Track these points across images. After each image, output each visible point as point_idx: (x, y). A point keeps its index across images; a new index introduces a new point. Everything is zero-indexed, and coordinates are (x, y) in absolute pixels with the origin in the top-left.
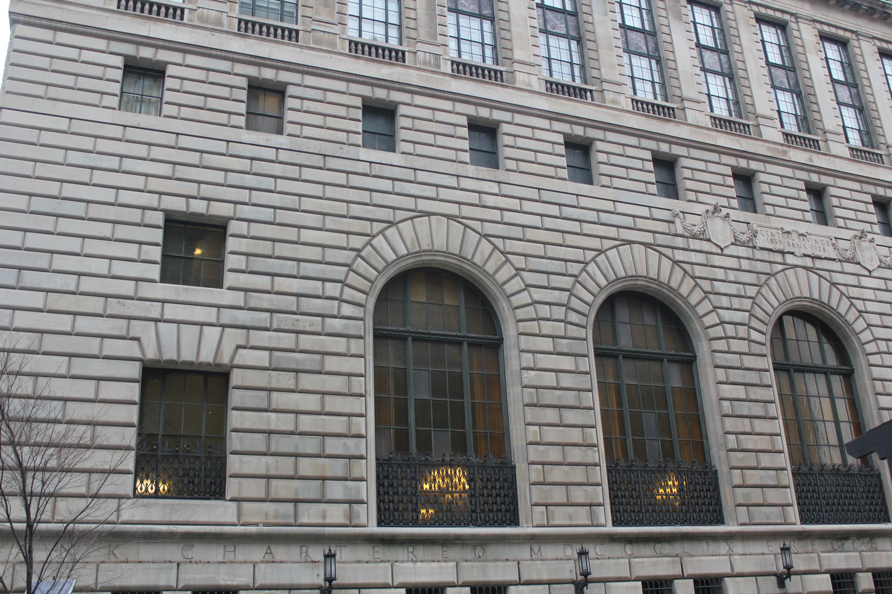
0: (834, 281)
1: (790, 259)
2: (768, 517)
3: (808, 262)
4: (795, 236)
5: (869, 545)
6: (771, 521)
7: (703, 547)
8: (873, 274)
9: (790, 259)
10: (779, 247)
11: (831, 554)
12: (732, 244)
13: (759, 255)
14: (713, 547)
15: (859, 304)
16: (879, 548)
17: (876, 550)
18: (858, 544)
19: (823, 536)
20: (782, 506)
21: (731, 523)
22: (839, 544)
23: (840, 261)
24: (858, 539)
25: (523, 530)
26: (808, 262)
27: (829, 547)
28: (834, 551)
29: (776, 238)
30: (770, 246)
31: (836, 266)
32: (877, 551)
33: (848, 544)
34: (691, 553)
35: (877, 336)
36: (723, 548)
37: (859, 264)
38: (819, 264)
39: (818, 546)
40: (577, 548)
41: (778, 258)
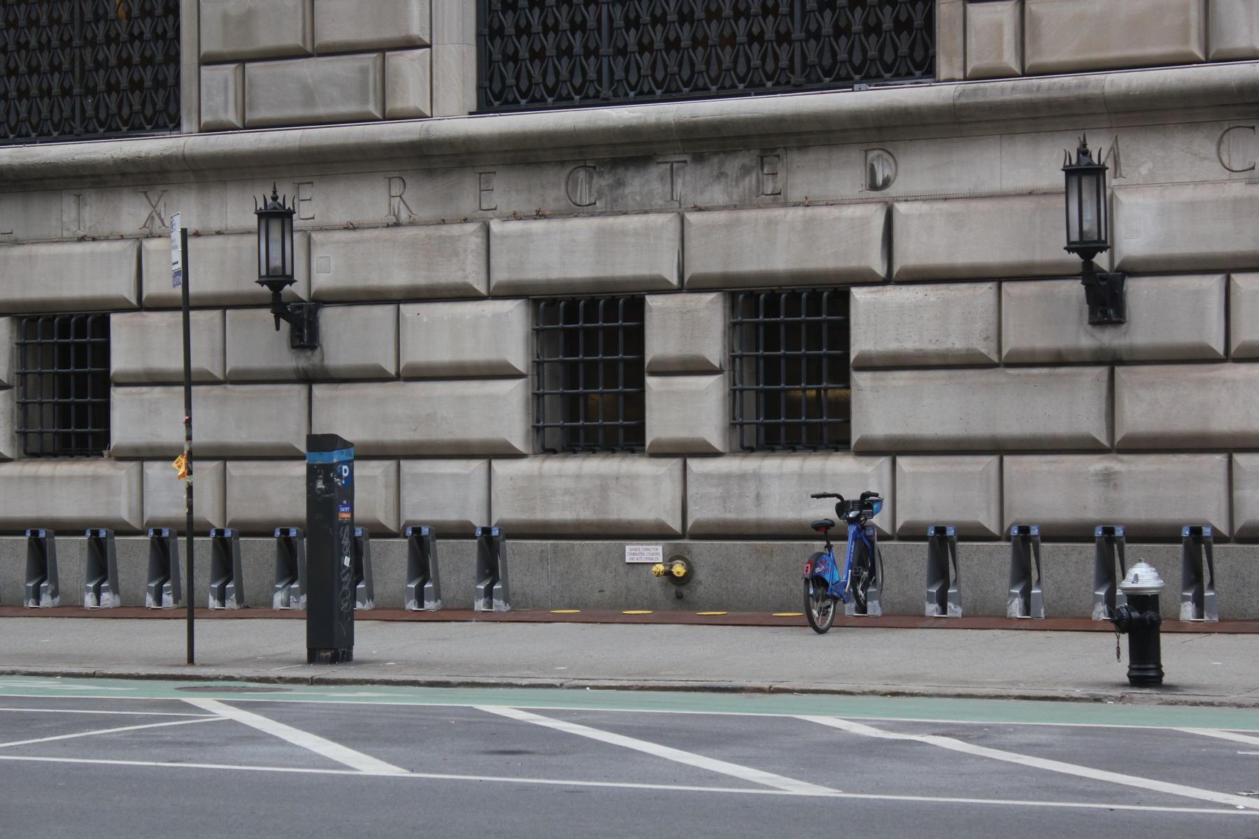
2: (309, 95)
5: (750, 181)
6: (321, 111)
7: (66, 213)
11: (538, 226)
14: (92, 212)
16: (796, 194)
17: (778, 199)
18: (692, 183)
19: (523, 155)
20: (381, 49)
21: (185, 126)
22: (603, 182)
24: (699, 158)
25: (183, 143)
27: (554, 195)
28: (575, 210)
32: (786, 204)
33: (644, 183)
34: (19, 234)
36: (131, 213)
39: (505, 192)
40: (259, 195)
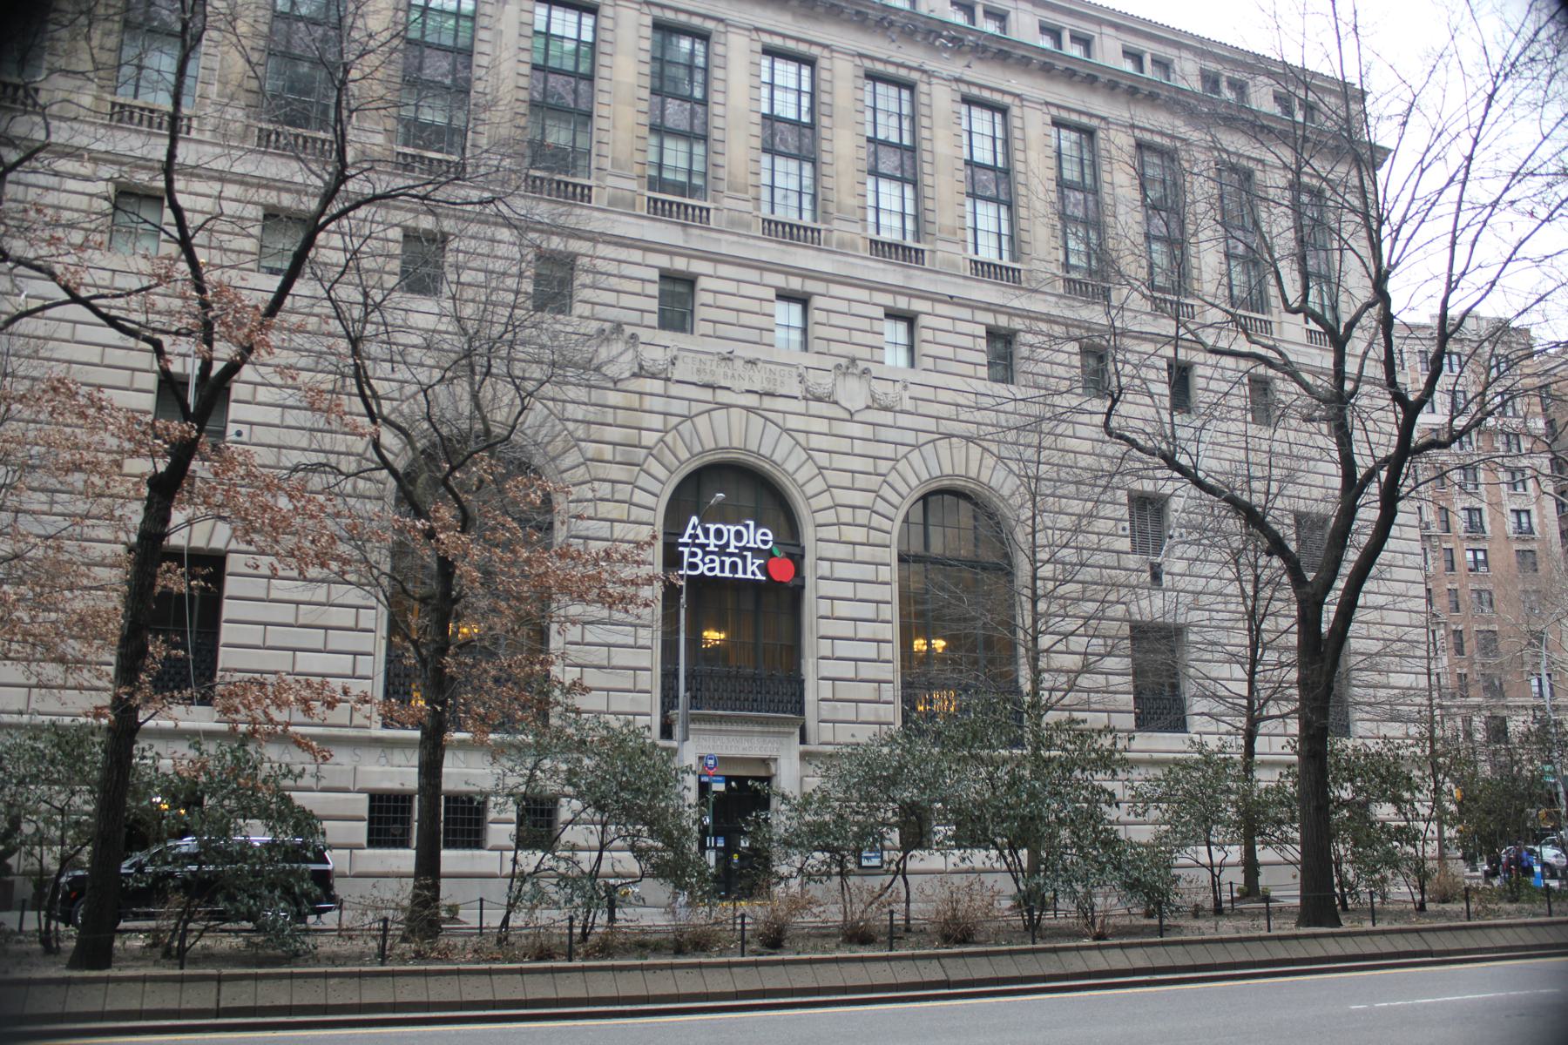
0: (790, 425)
1: (723, 397)
3: (752, 400)
4: (739, 364)
8: (856, 417)
9: (723, 397)
10: (707, 379)
12: (634, 375)
13: (675, 390)
15: (822, 459)
23: (805, 398)
26: (752, 400)
29: (708, 368)
30: (695, 379)
31: (799, 406)
35: (838, 501)
37: (836, 403)
38: (767, 402)
41: (707, 394)
